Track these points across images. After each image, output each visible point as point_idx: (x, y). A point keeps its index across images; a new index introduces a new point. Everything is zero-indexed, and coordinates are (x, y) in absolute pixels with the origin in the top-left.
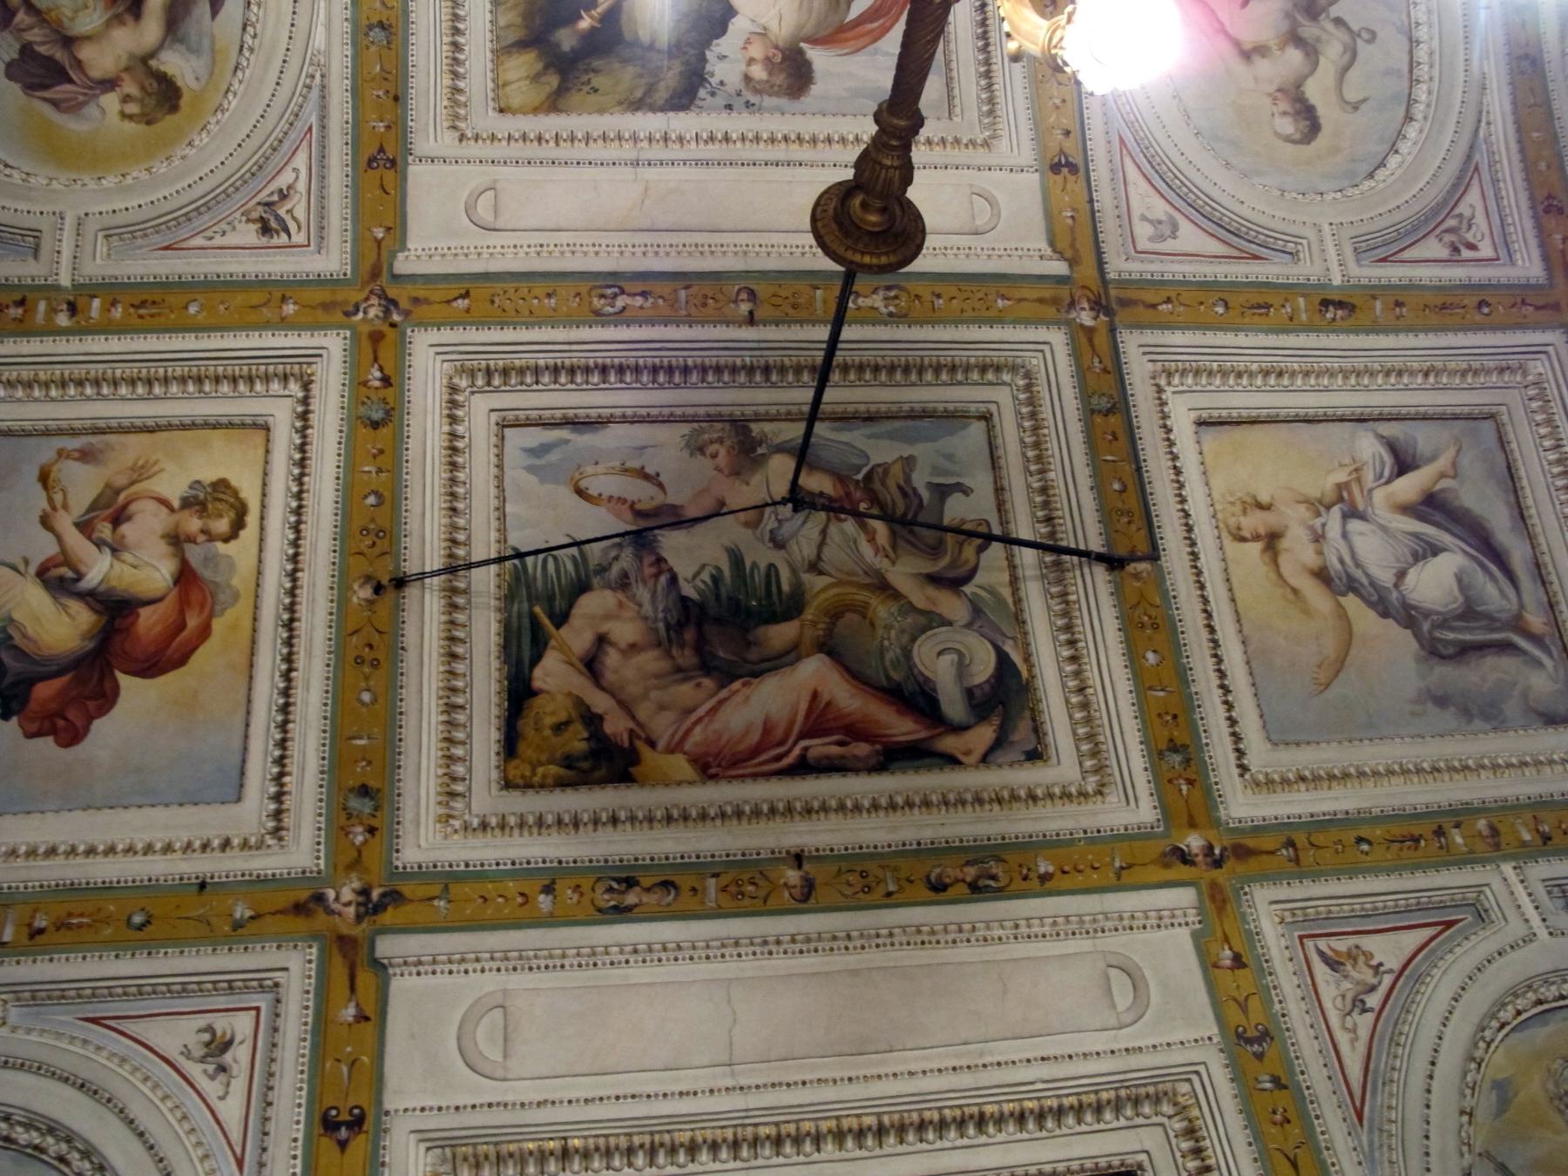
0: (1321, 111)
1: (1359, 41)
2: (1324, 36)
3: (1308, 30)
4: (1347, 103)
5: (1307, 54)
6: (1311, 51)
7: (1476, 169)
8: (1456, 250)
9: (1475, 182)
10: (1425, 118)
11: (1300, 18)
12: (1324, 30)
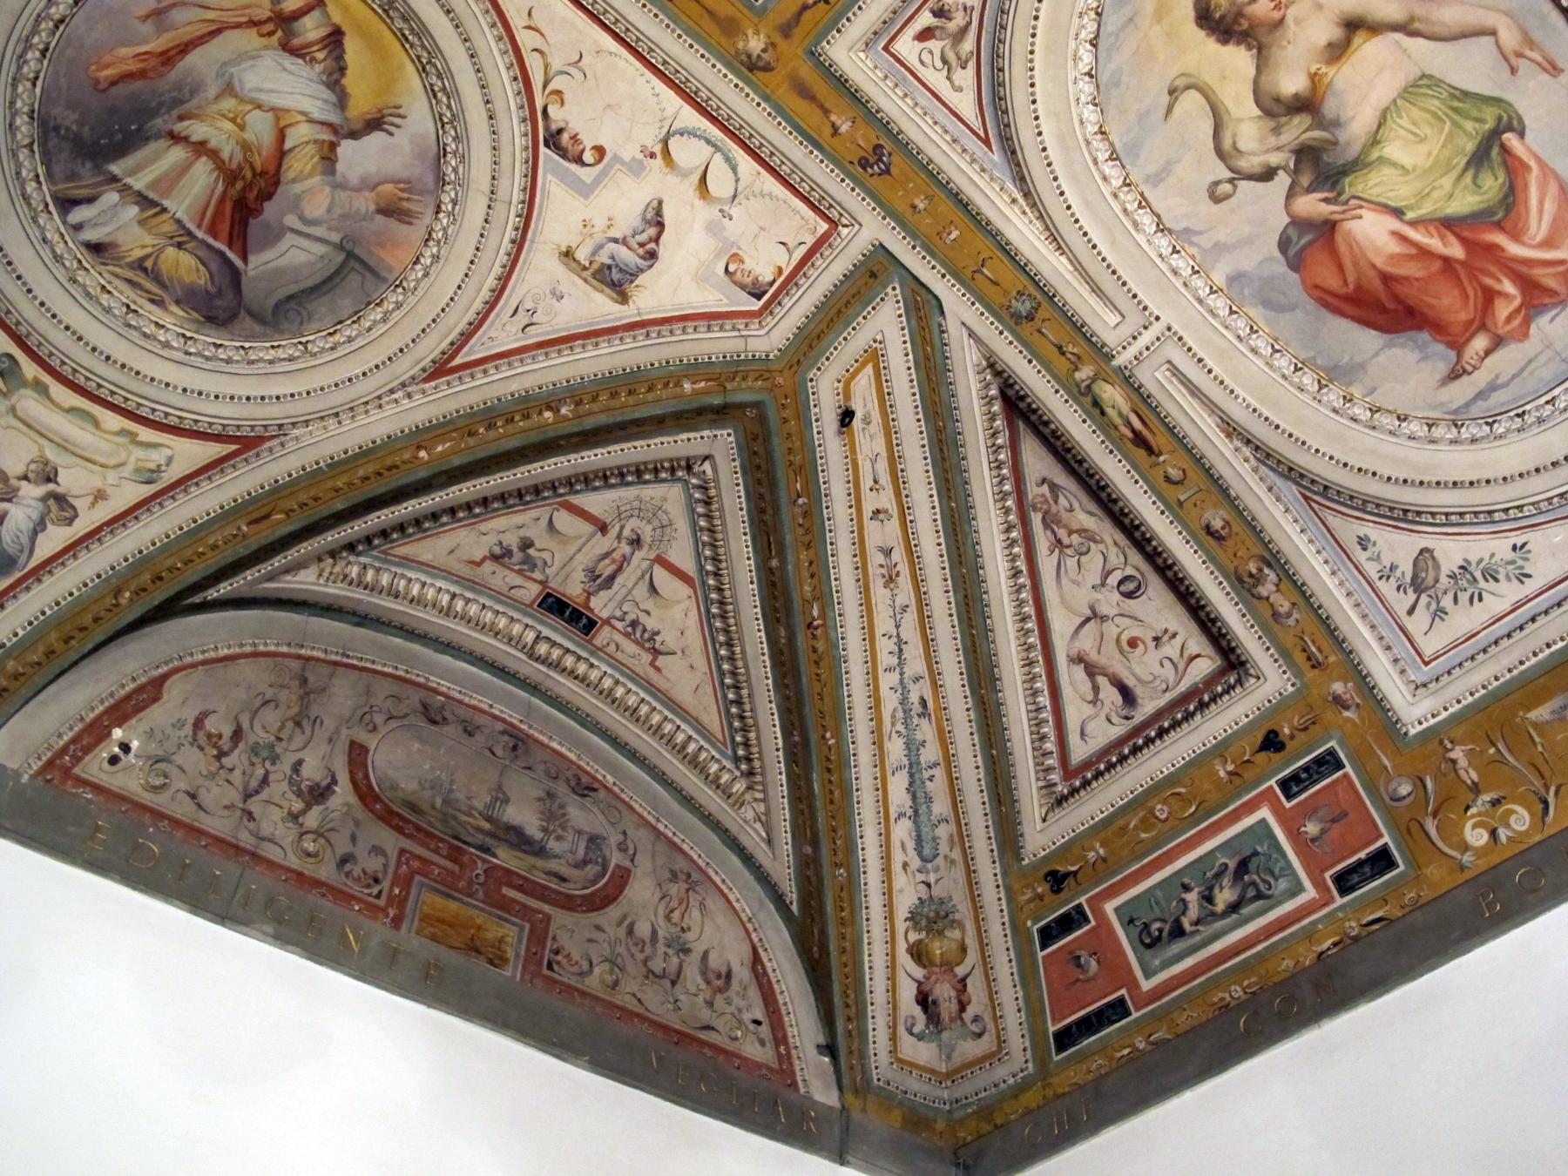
0: (1211, 45)
1: (1229, 174)
2: (1273, 141)
3: (1297, 129)
4: (1188, 87)
5: (1278, 100)
6: (1276, 108)
7: (987, 142)
8: (940, 13)
9: (976, 124)
10: (1088, 143)
11: (1317, 134)
12: (1278, 149)
